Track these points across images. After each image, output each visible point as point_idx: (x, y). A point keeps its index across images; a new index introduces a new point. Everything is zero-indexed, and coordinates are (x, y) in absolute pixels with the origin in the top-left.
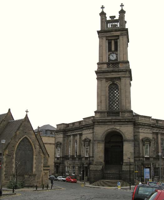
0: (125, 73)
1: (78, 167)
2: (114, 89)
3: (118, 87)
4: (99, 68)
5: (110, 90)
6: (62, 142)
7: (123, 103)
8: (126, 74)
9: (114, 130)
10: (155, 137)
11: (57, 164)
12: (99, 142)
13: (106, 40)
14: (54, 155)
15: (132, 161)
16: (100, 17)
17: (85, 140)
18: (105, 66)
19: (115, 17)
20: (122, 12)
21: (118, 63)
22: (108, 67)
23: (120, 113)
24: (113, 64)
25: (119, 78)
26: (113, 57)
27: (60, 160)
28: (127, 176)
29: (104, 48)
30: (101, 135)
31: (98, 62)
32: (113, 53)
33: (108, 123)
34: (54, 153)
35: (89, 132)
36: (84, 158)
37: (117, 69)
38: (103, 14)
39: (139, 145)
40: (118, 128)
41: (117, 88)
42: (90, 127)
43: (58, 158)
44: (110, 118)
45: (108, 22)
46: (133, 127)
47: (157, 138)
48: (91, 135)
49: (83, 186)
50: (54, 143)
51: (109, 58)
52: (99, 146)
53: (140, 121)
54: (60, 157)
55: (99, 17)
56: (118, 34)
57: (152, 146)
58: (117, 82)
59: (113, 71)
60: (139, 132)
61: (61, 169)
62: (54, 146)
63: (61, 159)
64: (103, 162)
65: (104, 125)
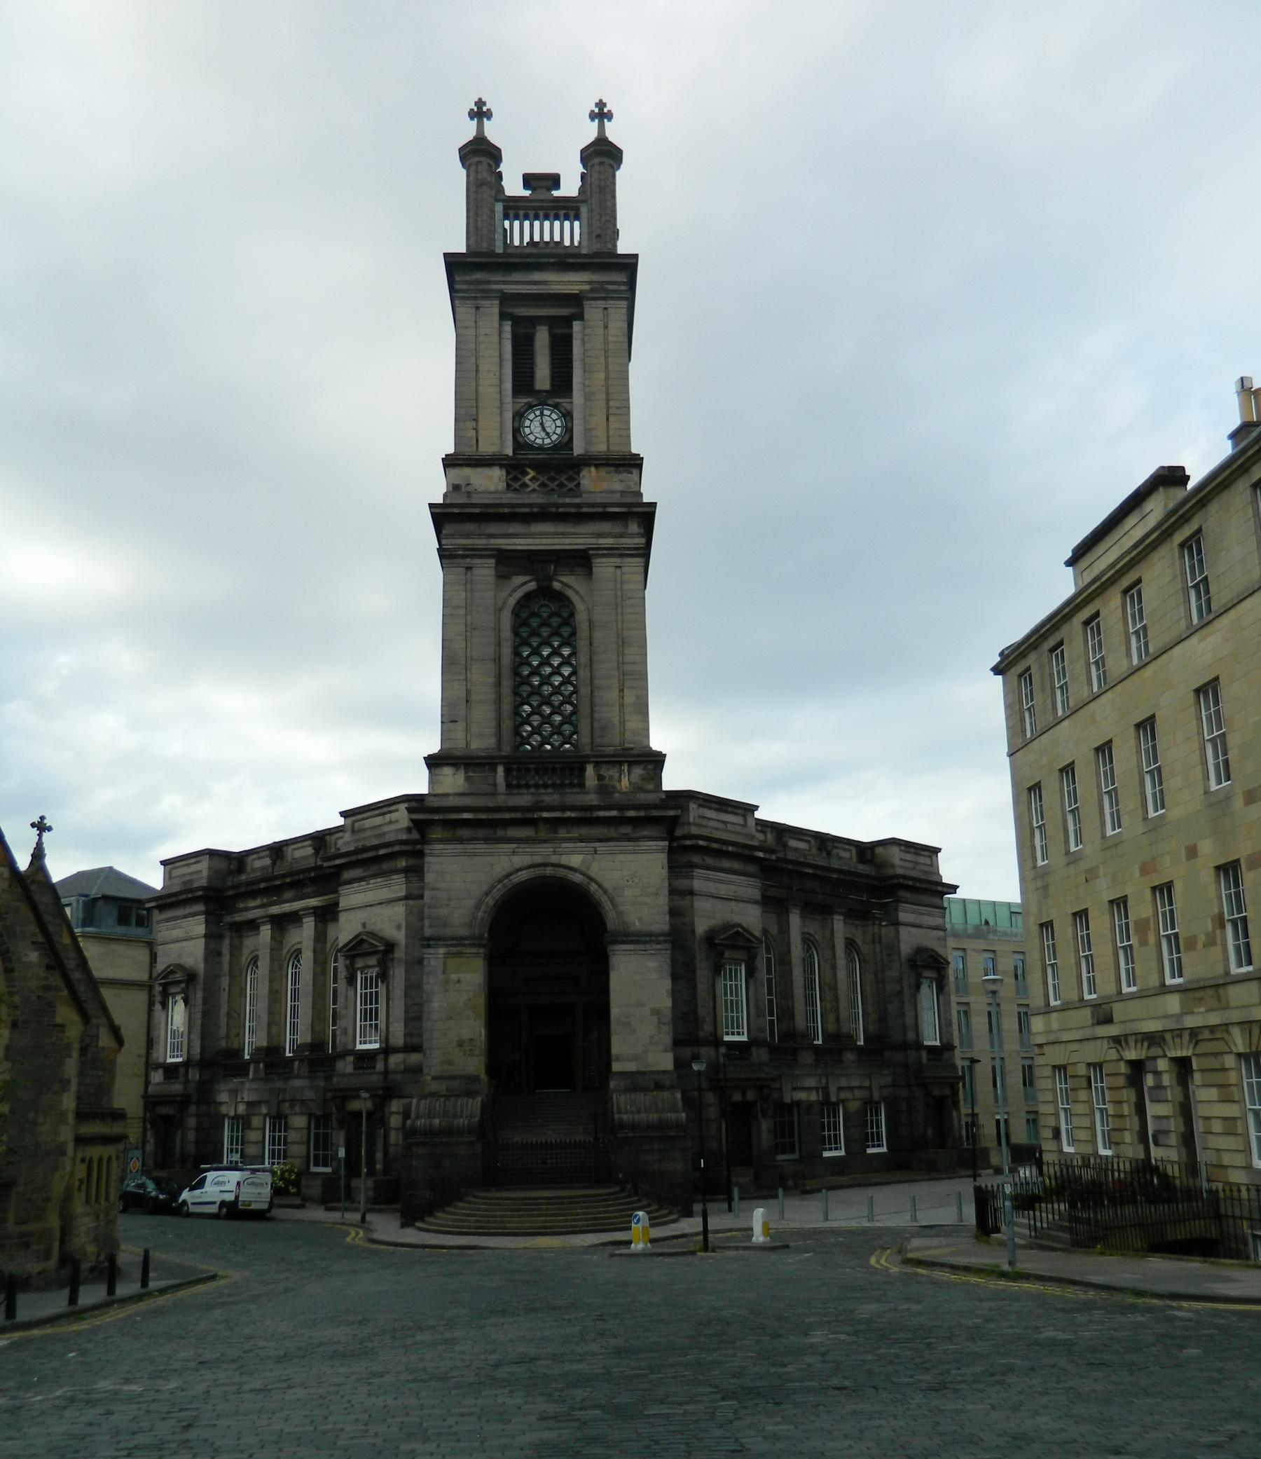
1: (310, 1116)
2: (545, 624)
3: (572, 615)
4: (455, 488)
5: (524, 632)
6: (200, 967)
8: (621, 536)
9: (549, 871)
10: (774, 929)
11: (162, 1110)
12: (457, 942)
13: (503, 316)
14: (143, 1052)
15: (666, 1062)
16: (463, 172)
17: (357, 948)
19: (554, 180)
20: (602, 157)
21: (576, 465)
22: (517, 485)
23: (590, 770)
24: (540, 467)
25: (581, 561)
27: (186, 1082)
29: (489, 365)
30: (471, 903)
31: (451, 450)
32: (544, 404)
33: (513, 832)
34: (144, 1039)
35: (385, 894)
36: (350, 1059)
37: (568, 500)
39: (694, 972)
40: (574, 858)
41: (569, 619)
42: (386, 866)
43: (171, 1071)
44: (524, 799)
46: (662, 858)
47: (784, 931)
48: (399, 910)
49: (355, 1237)
50: (144, 977)
51: (516, 431)
52: (454, 977)
53: (695, 824)
54: (186, 1064)
55: (459, 176)
56: (574, 289)
57: (762, 974)
59: (543, 515)
61: (191, 1136)
62: (141, 997)
63: (194, 1075)
64: (484, 1077)
65: (487, 840)
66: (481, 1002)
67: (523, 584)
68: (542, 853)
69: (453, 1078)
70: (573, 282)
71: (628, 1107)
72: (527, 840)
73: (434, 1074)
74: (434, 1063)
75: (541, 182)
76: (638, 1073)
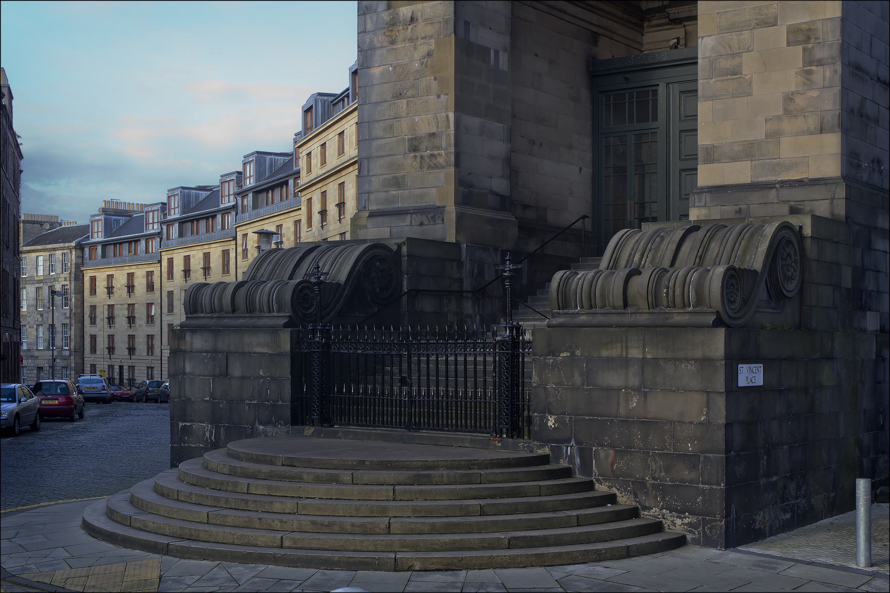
28: (613, 379)
64: (451, 210)
69: (400, 213)
73: (373, 207)
76: (754, 187)
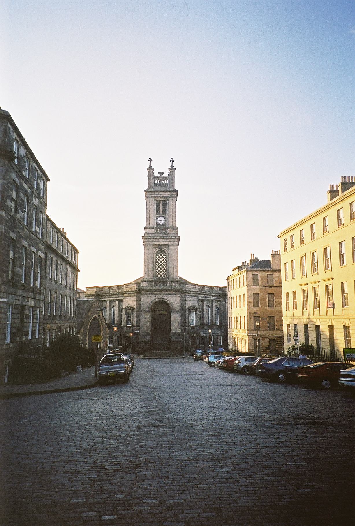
0: (174, 240)
4: (146, 233)
7: (171, 272)
13: (154, 200)
17: (127, 309)
18: (153, 231)
20: (172, 169)
21: (167, 229)
25: (168, 245)
26: (161, 221)
29: (152, 210)
33: (155, 293)
38: (150, 169)
40: (165, 297)
44: (158, 287)
45: (157, 178)
48: (135, 302)
51: (156, 221)
55: (147, 172)
56: (167, 196)
58: (165, 248)
59: (161, 238)
60: (185, 300)
66: (150, 321)
67: (157, 249)
68: (160, 296)
70: (167, 194)
71: (172, 338)
72: (157, 294)
74: (142, 330)
75: (161, 173)
